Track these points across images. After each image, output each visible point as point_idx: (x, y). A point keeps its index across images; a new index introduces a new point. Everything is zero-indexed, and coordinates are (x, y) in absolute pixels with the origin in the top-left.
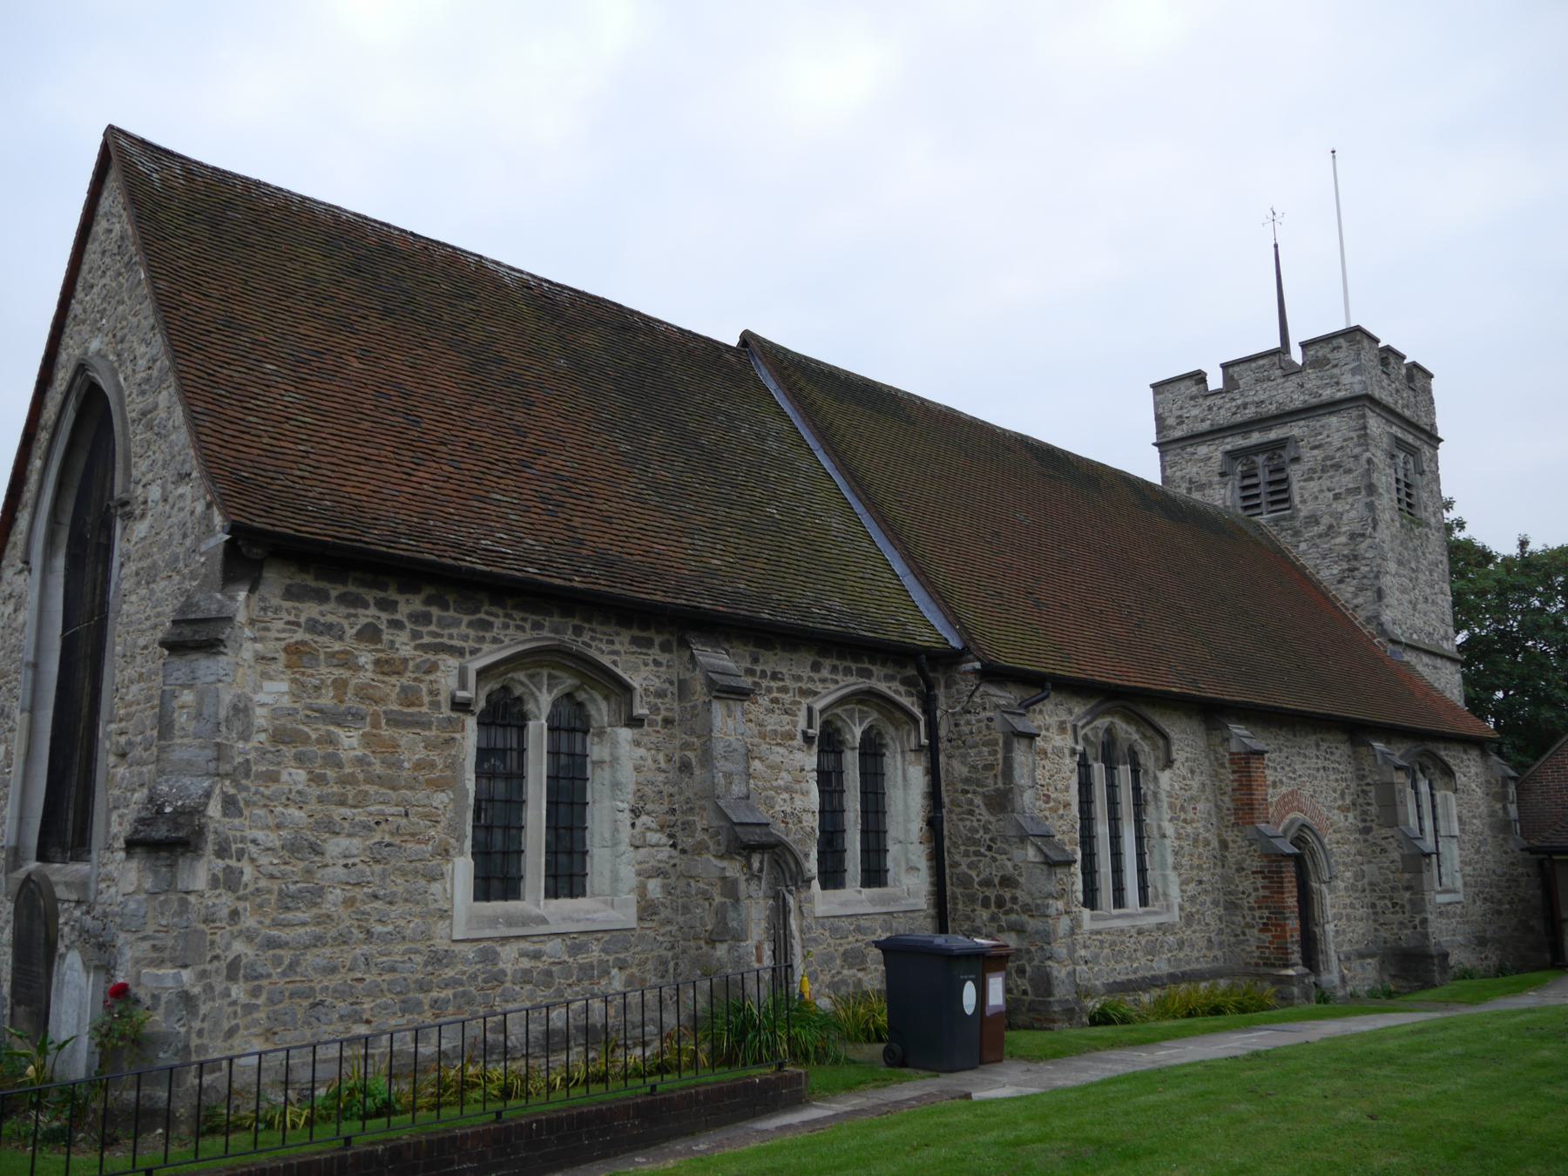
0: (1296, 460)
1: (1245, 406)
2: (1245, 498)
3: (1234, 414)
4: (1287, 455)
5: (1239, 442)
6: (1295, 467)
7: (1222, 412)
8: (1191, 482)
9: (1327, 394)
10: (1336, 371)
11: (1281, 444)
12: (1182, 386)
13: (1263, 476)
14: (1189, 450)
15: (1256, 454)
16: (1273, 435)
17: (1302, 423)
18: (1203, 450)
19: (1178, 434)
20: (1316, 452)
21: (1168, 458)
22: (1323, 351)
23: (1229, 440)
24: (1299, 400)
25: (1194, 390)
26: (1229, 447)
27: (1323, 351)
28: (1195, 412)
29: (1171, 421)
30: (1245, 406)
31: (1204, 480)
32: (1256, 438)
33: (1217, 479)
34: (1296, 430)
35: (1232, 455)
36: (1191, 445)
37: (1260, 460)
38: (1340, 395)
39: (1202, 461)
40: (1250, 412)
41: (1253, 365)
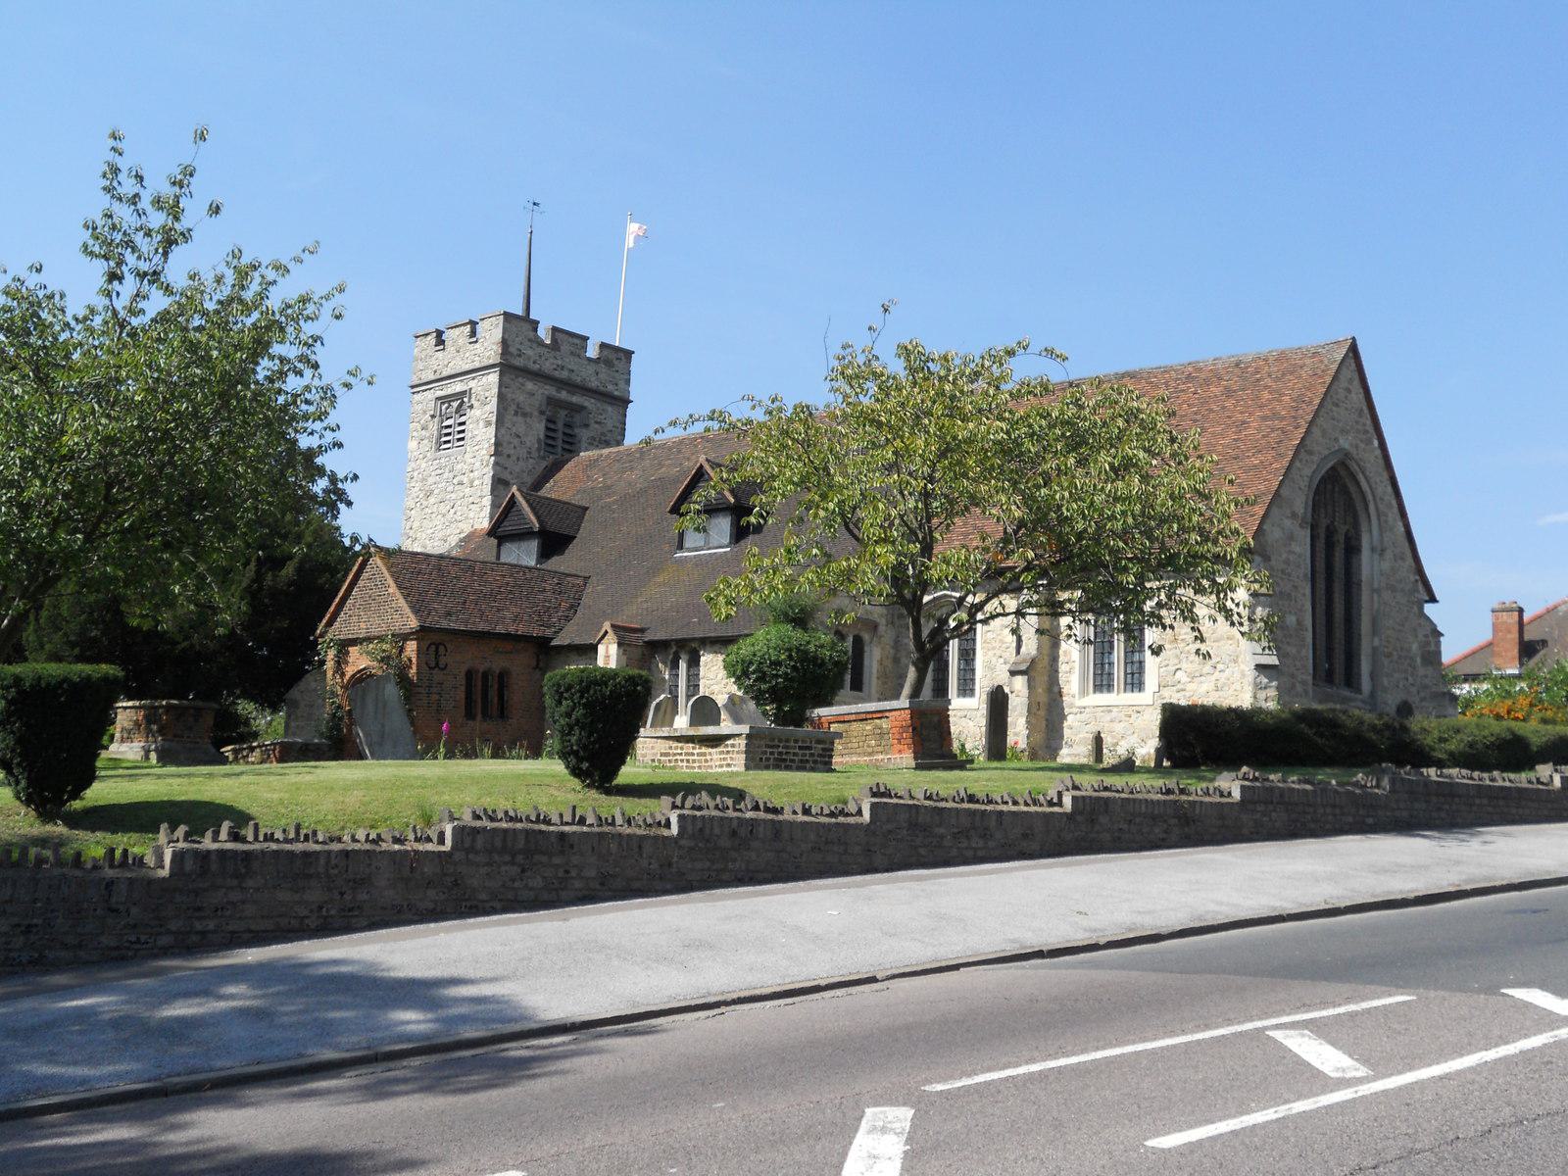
0: (587, 426)
1: (563, 368)
2: (547, 437)
3: (555, 369)
4: (577, 419)
5: (564, 395)
6: (584, 431)
7: (547, 364)
8: (518, 407)
9: (610, 388)
10: (616, 374)
11: (581, 409)
13: (560, 426)
14: (520, 380)
15: (561, 407)
16: (575, 399)
17: (593, 401)
18: (530, 386)
19: (518, 362)
20: (596, 426)
21: (504, 379)
22: (612, 356)
24: (594, 384)
25: (532, 334)
26: (546, 392)
27: (612, 356)
28: (530, 352)
29: (512, 350)
30: (563, 368)
31: (528, 410)
32: (564, 395)
33: (536, 413)
34: (588, 402)
35: (551, 401)
37: (563, 413)
38: (616, 393)
39: (528, 393)
40: (564, 374)
41: (570, 339)
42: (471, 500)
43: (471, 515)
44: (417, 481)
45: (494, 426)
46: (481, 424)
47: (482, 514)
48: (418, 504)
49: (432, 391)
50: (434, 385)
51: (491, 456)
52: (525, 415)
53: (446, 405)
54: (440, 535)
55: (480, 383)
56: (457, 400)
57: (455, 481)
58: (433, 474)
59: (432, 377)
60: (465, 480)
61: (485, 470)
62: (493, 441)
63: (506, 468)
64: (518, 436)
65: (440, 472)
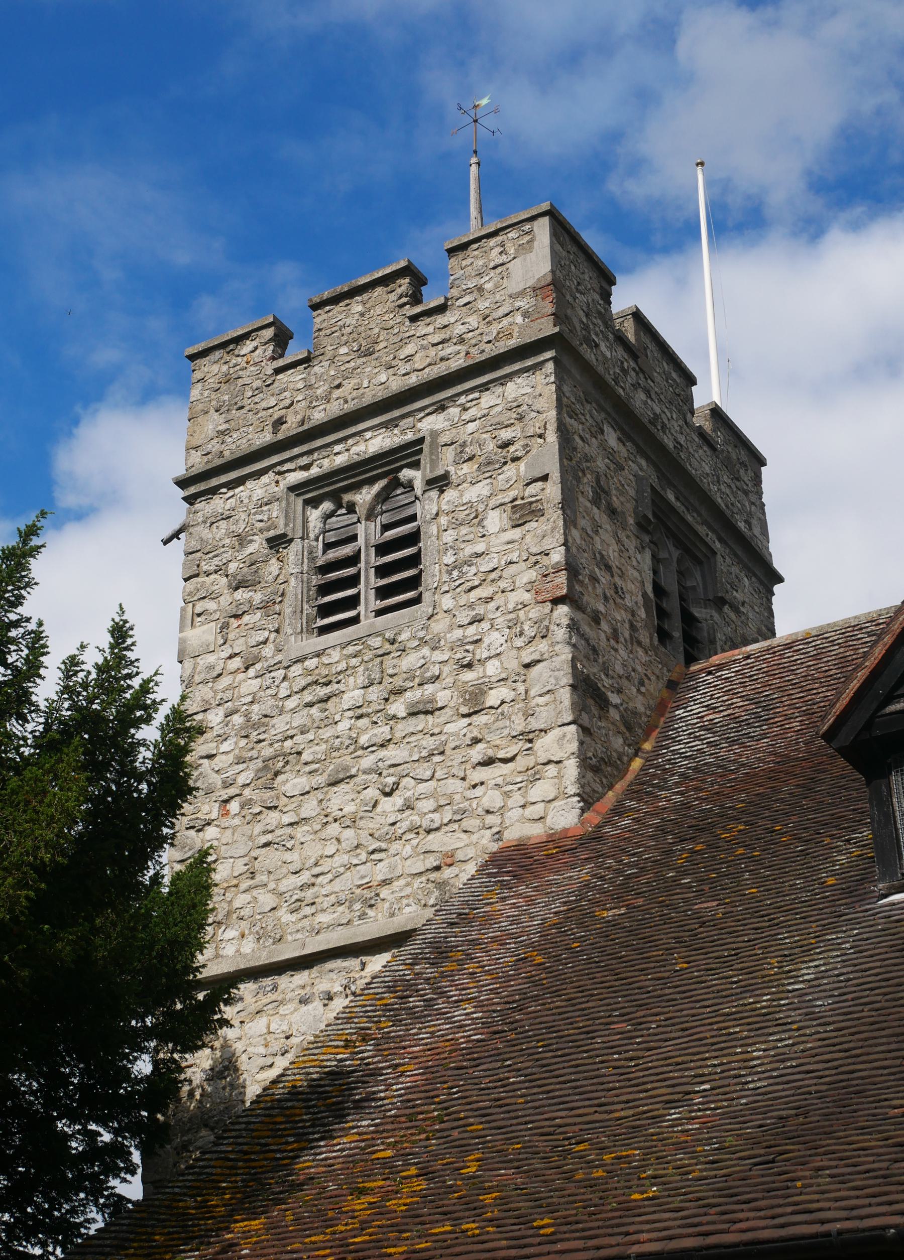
12: (588, 276)
18: (612, 438)
23: (643, 463)
36: (601, 409)
42: (477, 753)
43: (492, 798)
44: (222, 738)
45: (554, 518)
46: (494, 521)
47: (542, 789)
48: (234, 806)
49: (265, 479)
50: (275, 459)
51: (556, 601)
52: (612, 512)
53: (327, 506)
54: (350, 880)
55: (473, 412)
56: (371, 481)
57: (398, 707)
58: (291, 704)
59: (267, 437)
60: (443, 697)
61: (543, 646)
62: (558, 556)
63: (594, 650)
64: (608, 568)
65: (323, 692)
